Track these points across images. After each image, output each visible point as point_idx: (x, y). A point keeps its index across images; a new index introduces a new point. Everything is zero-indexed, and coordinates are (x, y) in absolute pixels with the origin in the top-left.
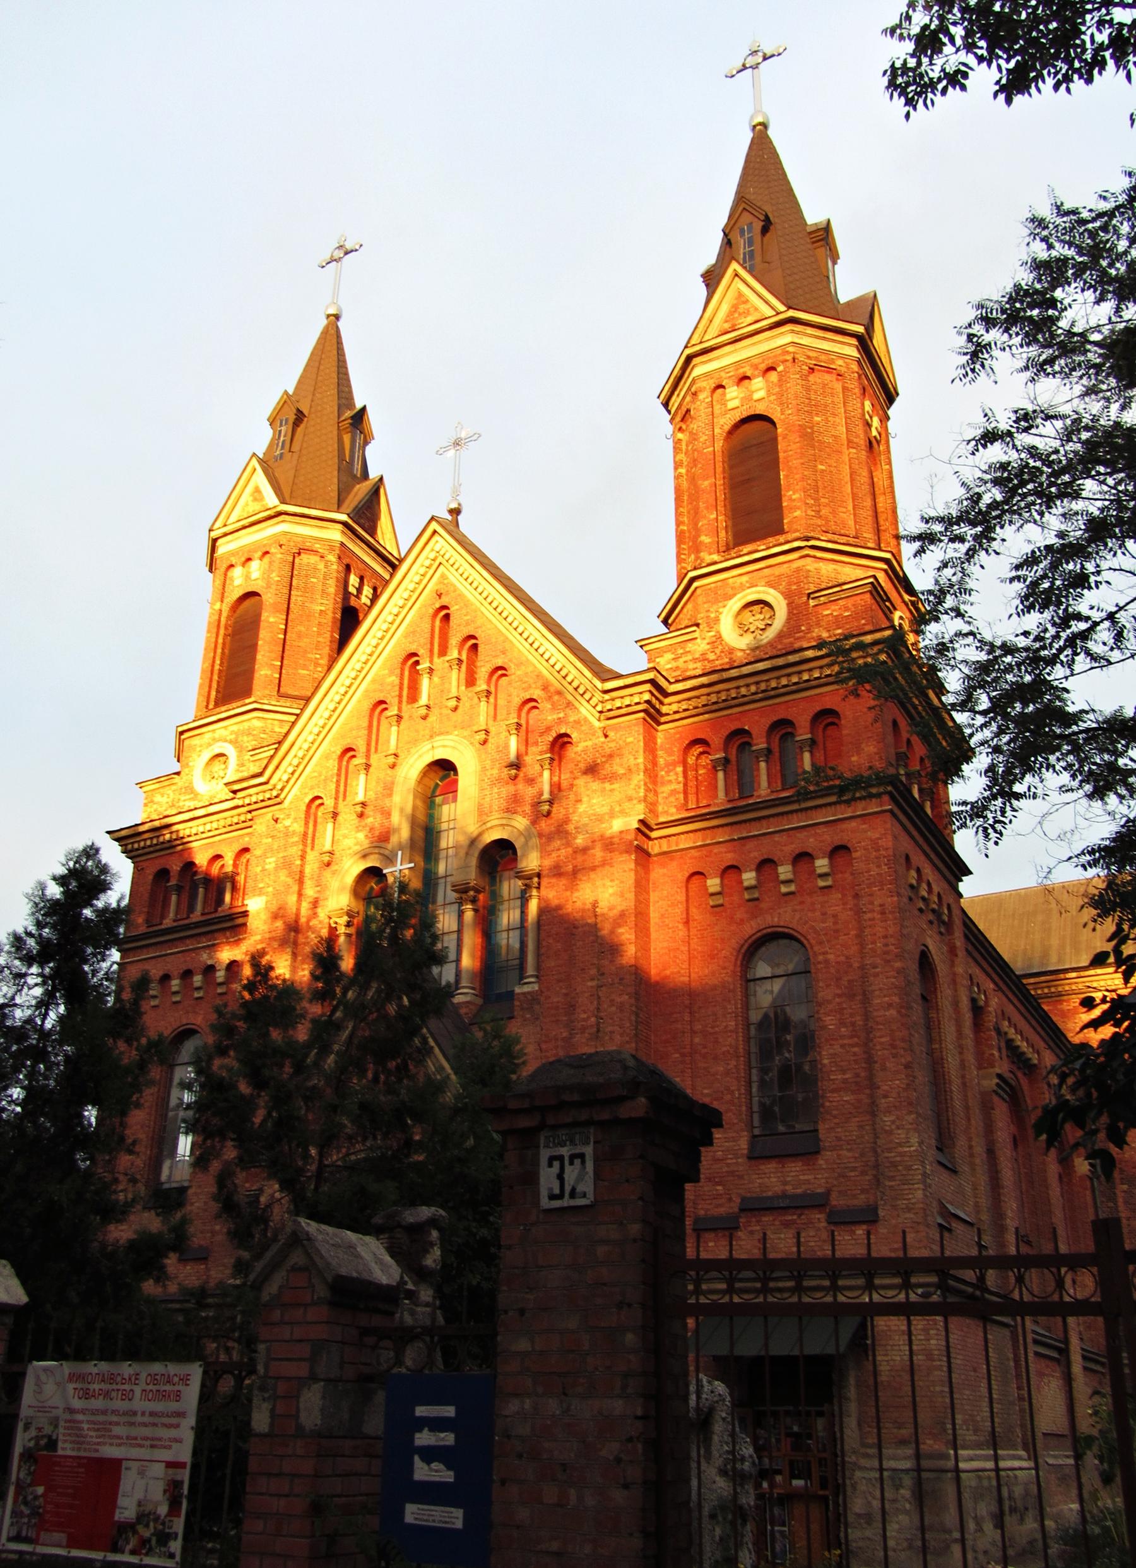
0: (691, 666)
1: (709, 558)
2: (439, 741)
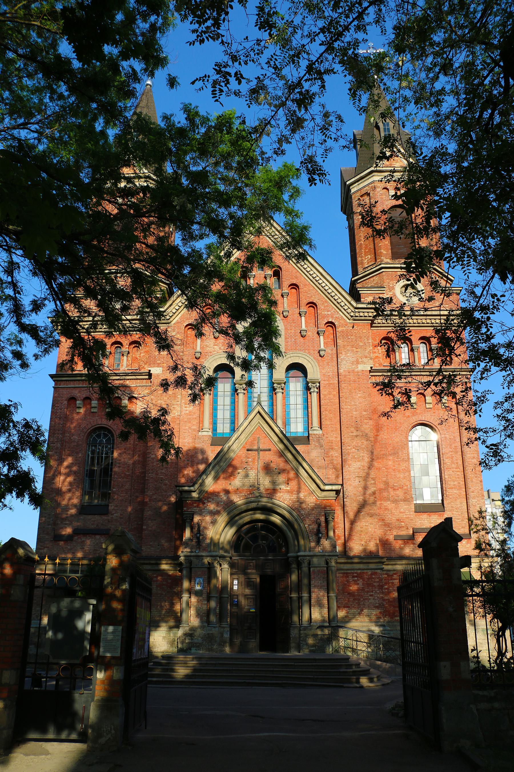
1: (386, 260)
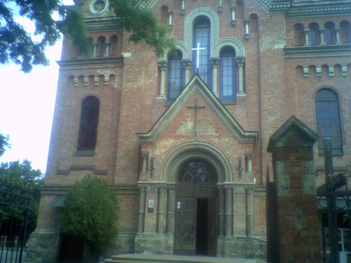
2: (202, 9)
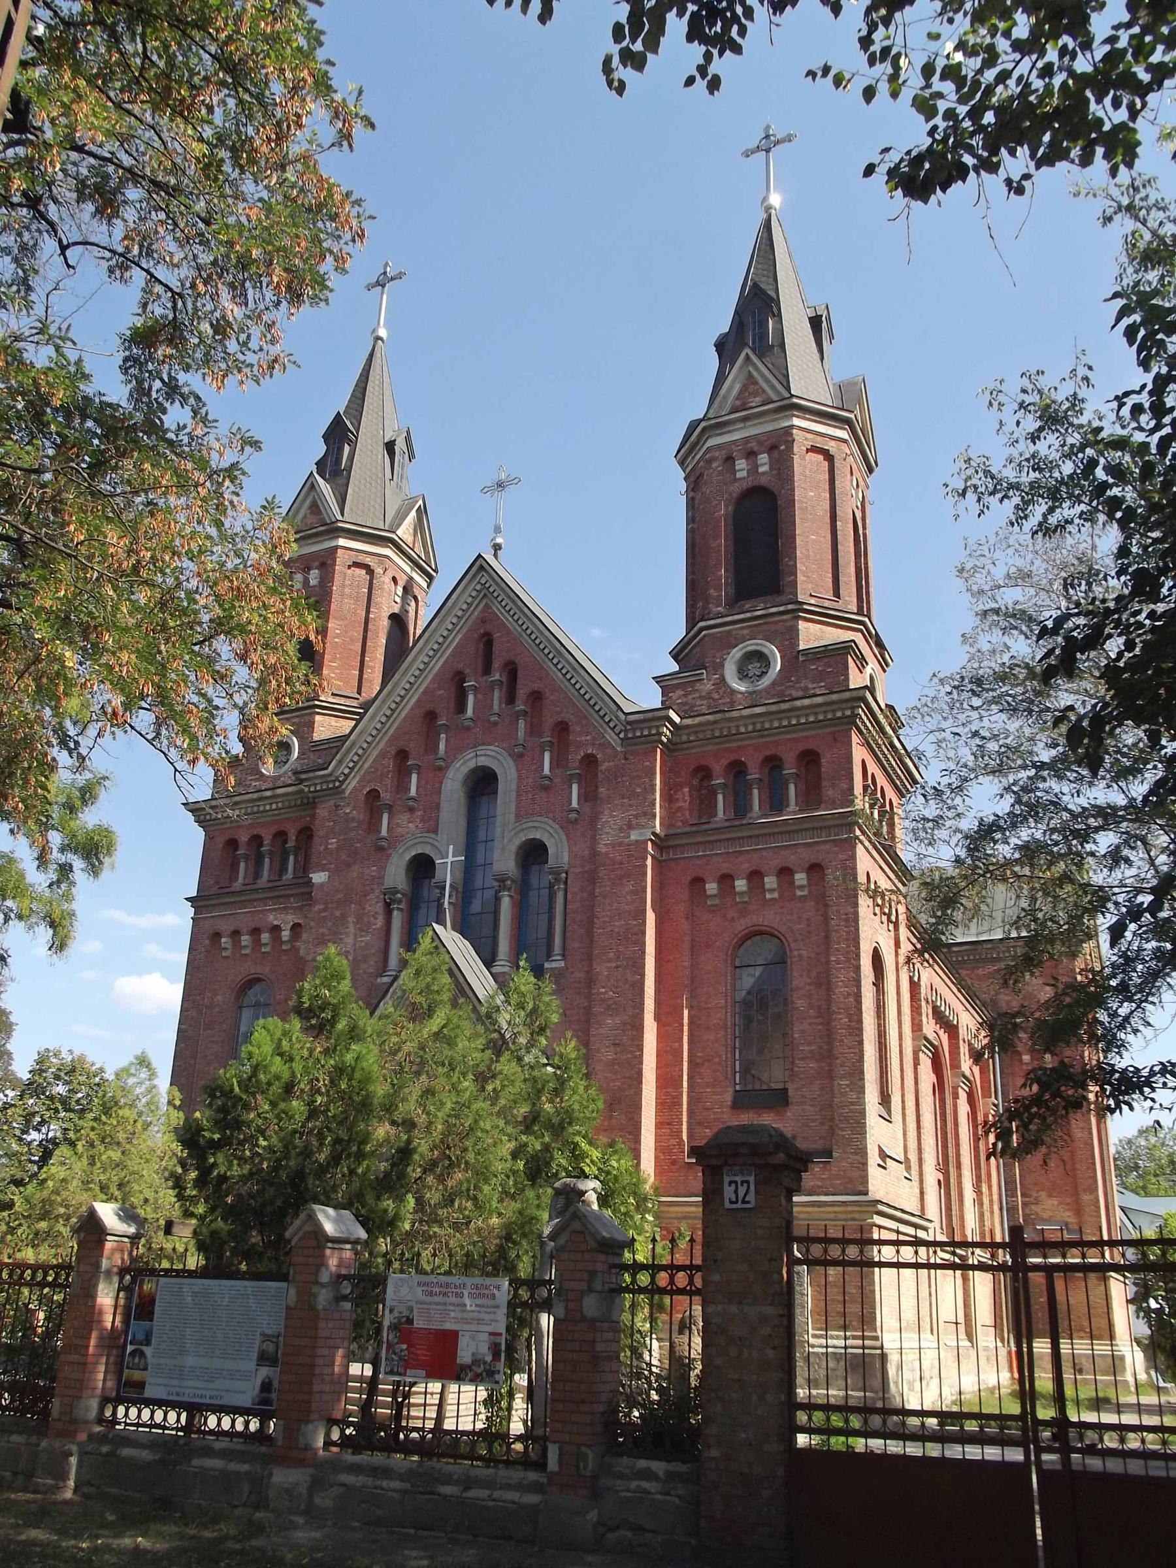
0: (698, 702)
